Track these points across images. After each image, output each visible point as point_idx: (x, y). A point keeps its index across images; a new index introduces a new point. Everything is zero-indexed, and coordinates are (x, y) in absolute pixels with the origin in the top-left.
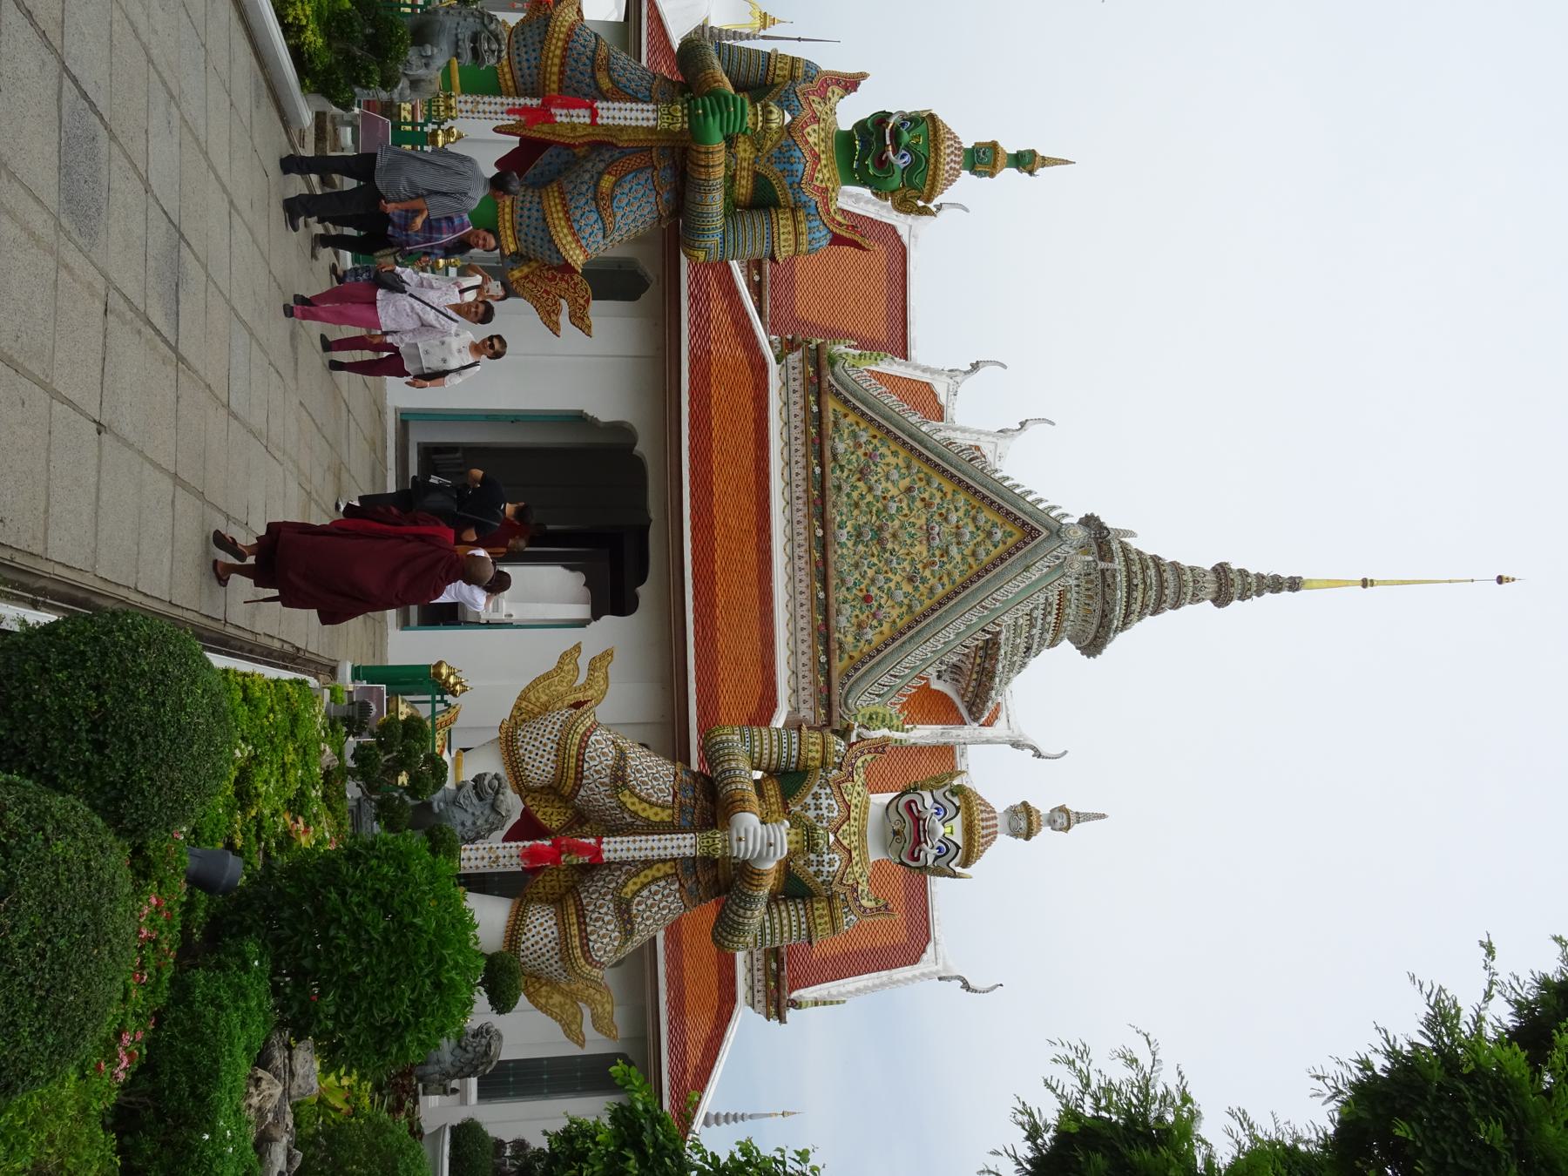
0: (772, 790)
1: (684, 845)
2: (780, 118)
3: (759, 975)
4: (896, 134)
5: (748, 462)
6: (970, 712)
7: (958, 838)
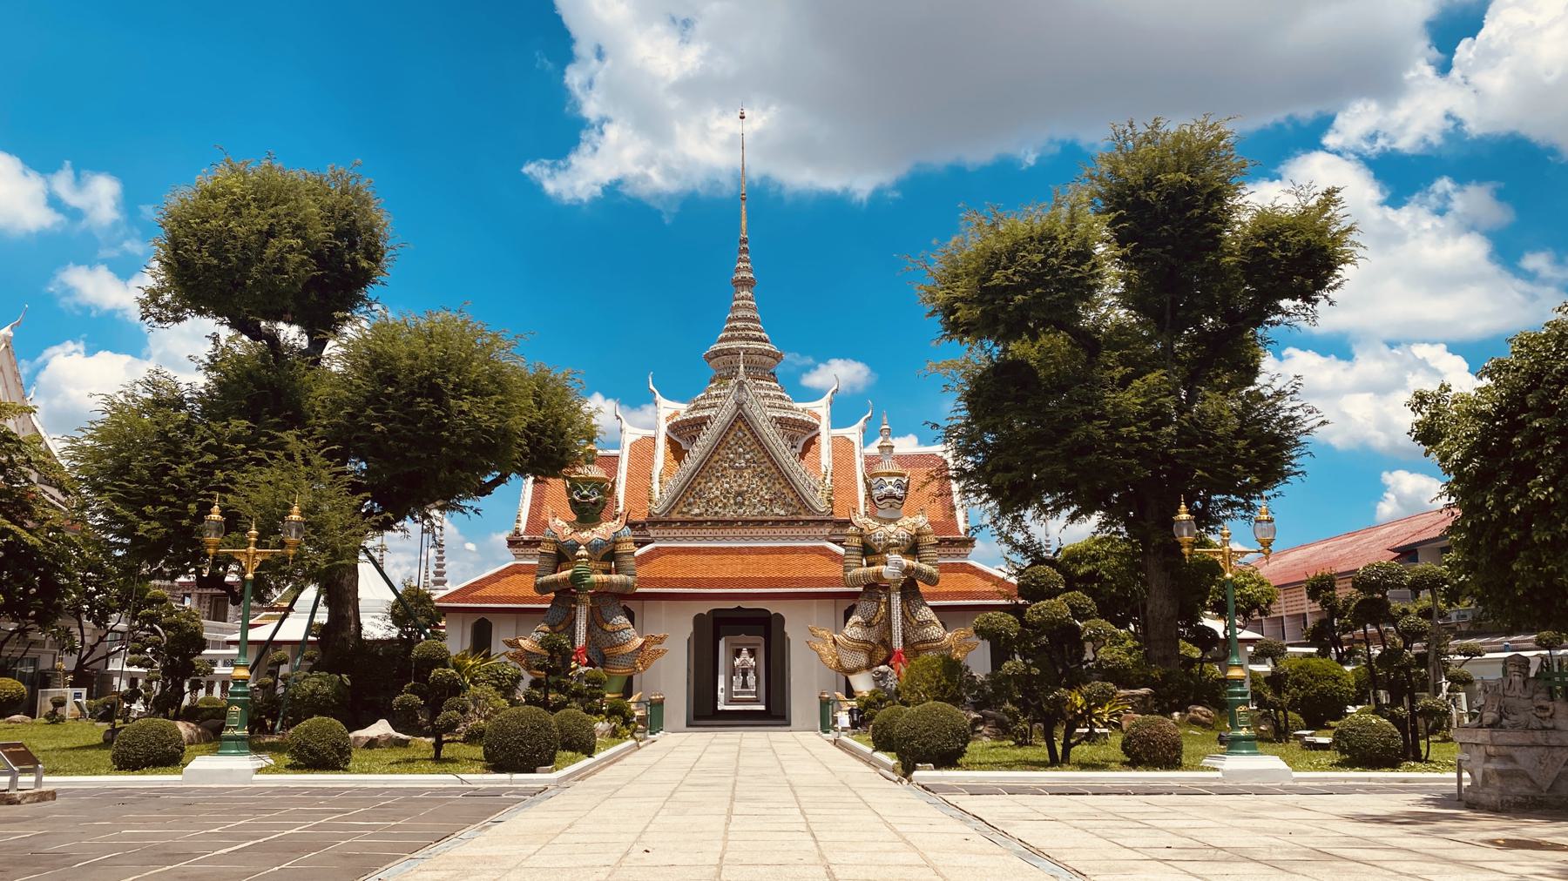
0: (872, 559)
1: (896, 600)
2: (582, 552)
3: (952, 551)
4: (583, 497)
5: (707, 559)
6: (811, 430)
7: (893, 480)
